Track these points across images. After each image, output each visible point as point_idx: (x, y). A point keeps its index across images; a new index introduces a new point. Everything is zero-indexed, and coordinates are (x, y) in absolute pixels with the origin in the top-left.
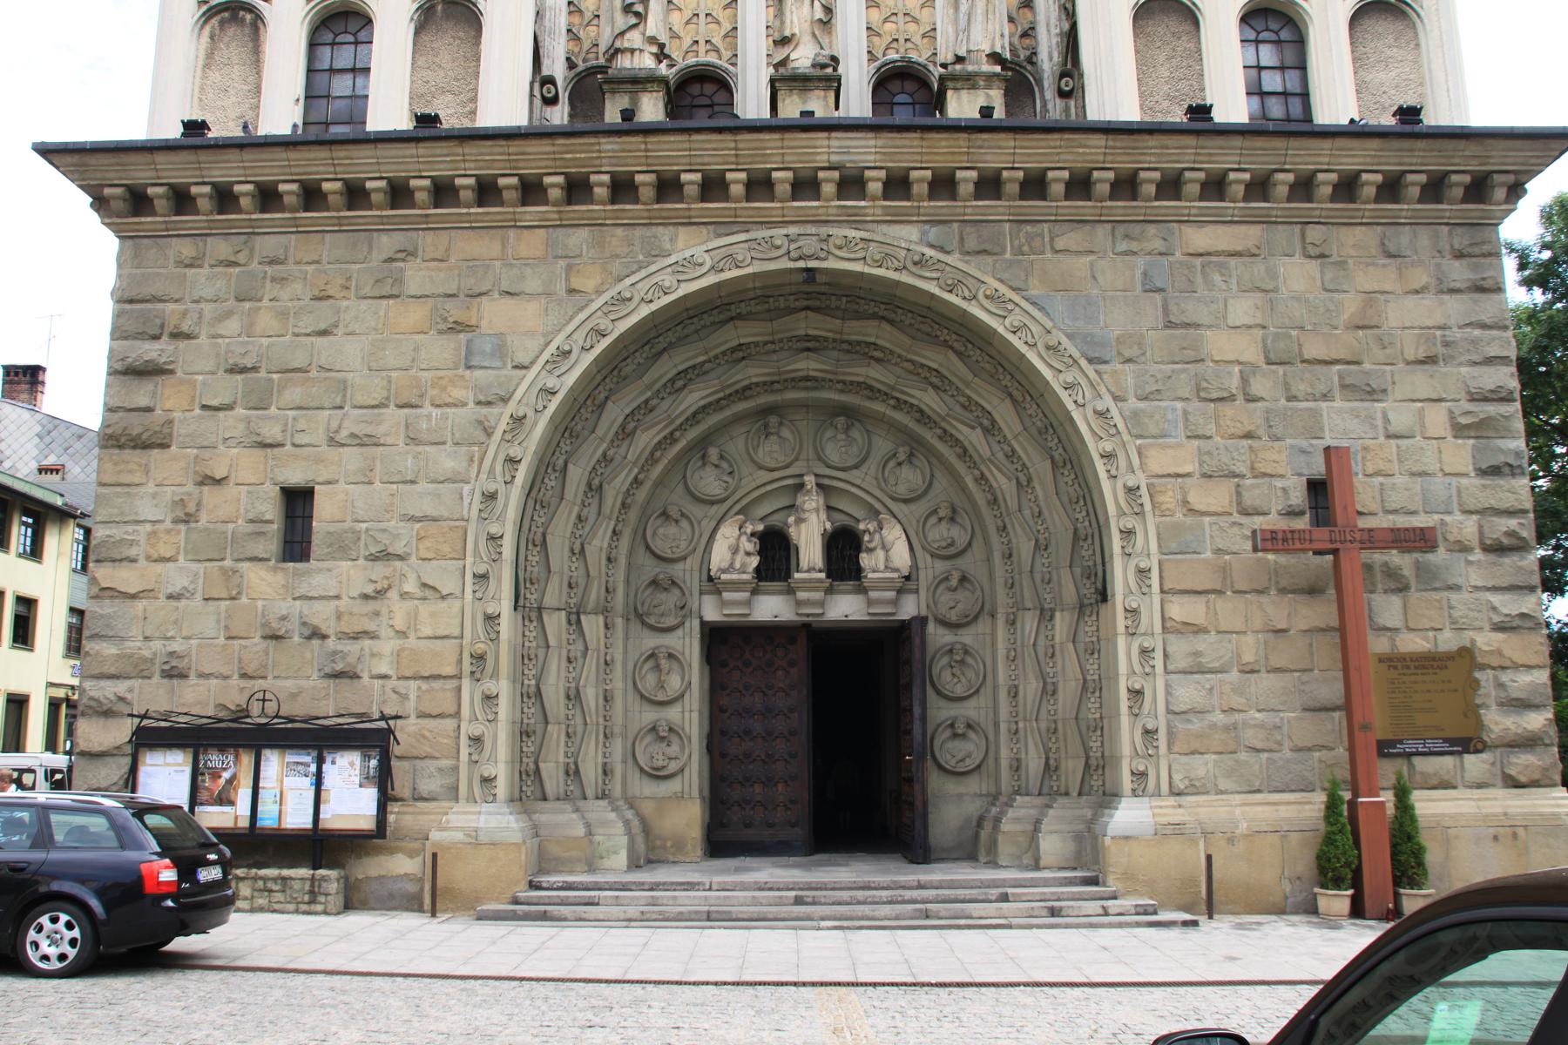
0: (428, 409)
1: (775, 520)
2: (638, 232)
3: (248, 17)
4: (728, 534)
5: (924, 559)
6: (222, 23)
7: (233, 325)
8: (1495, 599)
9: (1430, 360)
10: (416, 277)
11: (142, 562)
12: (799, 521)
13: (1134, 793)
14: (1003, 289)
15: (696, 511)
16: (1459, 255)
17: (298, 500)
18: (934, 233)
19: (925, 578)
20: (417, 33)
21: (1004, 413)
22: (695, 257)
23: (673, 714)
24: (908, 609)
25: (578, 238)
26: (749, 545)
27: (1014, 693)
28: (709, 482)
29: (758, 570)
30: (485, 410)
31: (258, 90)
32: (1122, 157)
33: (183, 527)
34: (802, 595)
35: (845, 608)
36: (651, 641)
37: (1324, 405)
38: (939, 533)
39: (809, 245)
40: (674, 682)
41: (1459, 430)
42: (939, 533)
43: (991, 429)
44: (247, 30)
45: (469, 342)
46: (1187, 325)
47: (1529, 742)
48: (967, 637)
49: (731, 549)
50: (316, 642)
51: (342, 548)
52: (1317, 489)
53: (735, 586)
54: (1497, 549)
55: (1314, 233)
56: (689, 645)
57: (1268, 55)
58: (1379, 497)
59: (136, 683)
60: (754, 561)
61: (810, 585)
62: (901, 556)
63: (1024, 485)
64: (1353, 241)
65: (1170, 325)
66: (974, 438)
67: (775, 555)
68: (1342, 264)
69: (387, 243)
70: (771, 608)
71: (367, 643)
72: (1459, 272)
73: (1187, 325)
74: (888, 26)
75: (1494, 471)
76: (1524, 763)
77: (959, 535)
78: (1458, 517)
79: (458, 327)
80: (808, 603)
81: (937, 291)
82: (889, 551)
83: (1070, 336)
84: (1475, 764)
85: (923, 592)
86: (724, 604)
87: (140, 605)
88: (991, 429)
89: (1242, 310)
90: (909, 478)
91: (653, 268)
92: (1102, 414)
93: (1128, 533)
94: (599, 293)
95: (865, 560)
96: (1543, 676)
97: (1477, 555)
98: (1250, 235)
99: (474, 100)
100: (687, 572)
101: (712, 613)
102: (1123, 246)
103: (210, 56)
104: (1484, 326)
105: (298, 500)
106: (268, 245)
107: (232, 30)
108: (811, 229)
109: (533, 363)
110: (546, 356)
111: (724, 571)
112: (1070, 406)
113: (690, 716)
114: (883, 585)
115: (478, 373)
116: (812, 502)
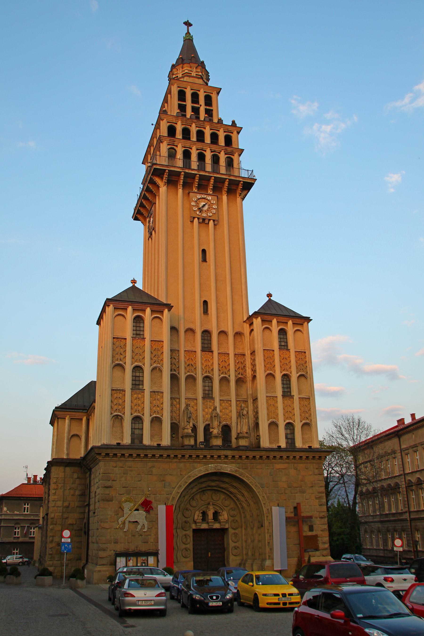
0: (158, 495)
1: (204, 509)
2: (192, 464)
3: (120, 417)
4: (197, 513)
5: (229, 517)
6: (115, 418)
7: (123, 479)
8: (320, 526)
9: (312, 487)
10: (155, 471)
11: (109, 522)
12: (209, 510)
13: (269, 559)
14: (248, 475)
15: (191, 508)
16: (317, 469)
18: (238, 465)
19: (230, 521)
20: (151, 423)
21: (246, 493)
22: (201, 469)
23: (188, 546)
24: (227, 526)
25: (182, 465)
26: (201, 515)
27: (246, 541)
28: (194, 503)
29: (202, 519)
30: (168, 495)
31: (123, 433)
32: (268, 454)
33: (116, 516)
34: (210, 524)
35: (217, 526)
36: (185, 532)
37: (296, 494)
38: (232, 513)
39: (219, 468)
40: (189, 540)
41: (316, 498)
42: (232, 513)
43: (243, 496)
44: (120, 420)
45: (164, 484)
46: (276, 481)
47: (325, 549)
48: (236, 531)
49: (198, 516)
50: (140, 537)
52: (295, 508)
53: (199, 522)
54: (321, 518)
55: (296, 465)
57: (289, 431)
58: (305, 512)
59: (109, 544)
60: (201, 518)
61: (211, 522)
62: (226, 516)
63: (249, 505)
64: (301, 466)
65: (273, 481)
66: (240, 497)
68: (299, 470)
69: (150, 464)
70: (204, 526)
71: (149, 536)
72: (316, 471)
73: (276, 481)
74: (224, 416)
75: (321, 505)
76: (325, 552)
78: (316, 512)
79: (163, 481)
80: (211, 525)
81: (238, 476)
82: (224, 516)
83: (258, 483)
84: (318, 553)
85: (229, 523)
86: (196, 525)
87: (109, 530)
88: (243, 496)
89: (284, 479)
90: (227, 503)
91: (194, 471)
92: (263, 497)
93: (267, 517)
94: (186, 475)
95: (220, 518)
96: (327, 538)
97: (319, 519)
98: (286, 465)
99: (161, 437)
100: (190, 520)
101: (194, 527)
102: (267, 468)
103: (113, 425)
104: (320, 481)
106: (129, 464)
107: (117, 420)
108: (219, 464)
109: (175, 487)
110: (177, 486)
111: (197, 520)
112: (259, 495)
113: (190, 546)
115: (166, 489)
116: (211, 507)
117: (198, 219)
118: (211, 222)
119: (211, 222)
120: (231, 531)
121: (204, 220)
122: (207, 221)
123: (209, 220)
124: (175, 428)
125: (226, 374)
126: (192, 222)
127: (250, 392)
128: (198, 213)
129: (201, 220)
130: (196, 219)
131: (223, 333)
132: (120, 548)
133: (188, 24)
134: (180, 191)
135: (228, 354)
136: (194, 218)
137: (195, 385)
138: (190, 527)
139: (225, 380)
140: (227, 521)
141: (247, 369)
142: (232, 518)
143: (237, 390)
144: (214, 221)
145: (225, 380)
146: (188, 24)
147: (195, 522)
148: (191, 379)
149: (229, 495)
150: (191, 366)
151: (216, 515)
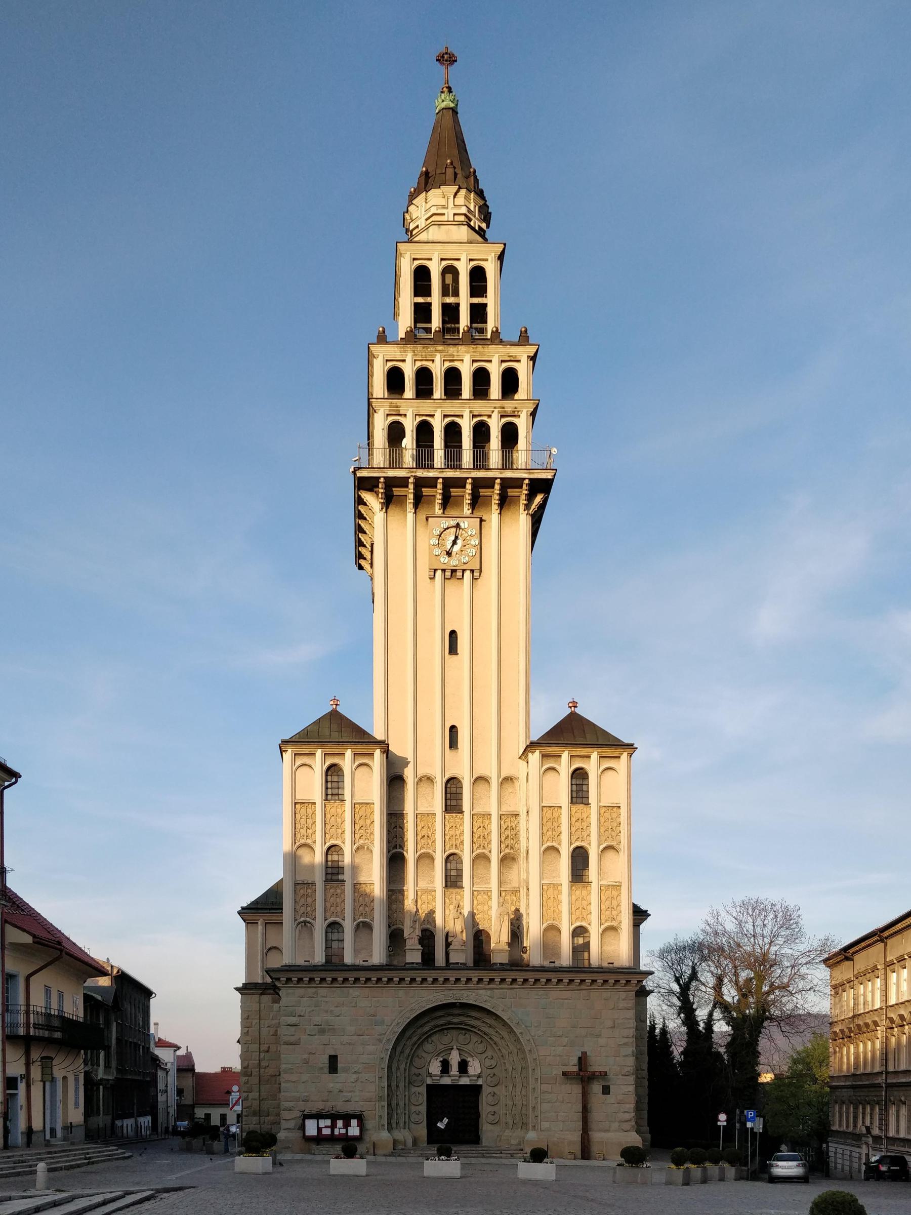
17: (333, 1060)
19: (483, 1075)
24: (480, 1082)
26: (440, 1064)
35: (465, 1081)
38: (488, 1063)
49: (435, 1067)
51: (346, 1070)
53: (436, 1075)
56: (423, 1090)
61: (454, 1076)
67: (445, 1067)
70: (446, 1081)
77: (493, 1063)
82: (474, 1067)
90: (481, 1048)
101: (429, 1082)
105: (333, 1060)
114: (474, 1076)
117: (444, 571)
118: (467, 573)
119: (467, 573)
120: (486, 1090)
121: (453, 571)
122: (459, 574)
123: (464, 571)
124: (395, 938)
125: (484, 847)
126: (433, 578)
127: (523, 876)
128: (442, 560)
129: (448, 574)
130: (439, 573)
131: (481, 780)
132: (310, 1108)
133: (447, 59)
134: (410, 516)
135: (490, 815)
136: (435, 570)
137: (433, 869)
138: (423, 1081)
139: (481, 859)
140: (479, 1076)
141: (521, 839)
142: (489, 1071)
143: (500, 873)
144: (472, 571)
145: (481, 859)
146: (447, 59)
147: (430, 1075)
148: (425, 858)
149: (483, 1036)
150: (425, 837)
151: (463, 1067)
